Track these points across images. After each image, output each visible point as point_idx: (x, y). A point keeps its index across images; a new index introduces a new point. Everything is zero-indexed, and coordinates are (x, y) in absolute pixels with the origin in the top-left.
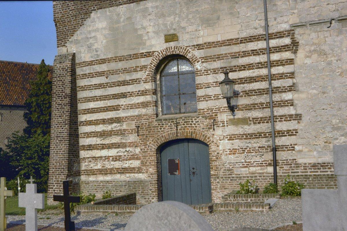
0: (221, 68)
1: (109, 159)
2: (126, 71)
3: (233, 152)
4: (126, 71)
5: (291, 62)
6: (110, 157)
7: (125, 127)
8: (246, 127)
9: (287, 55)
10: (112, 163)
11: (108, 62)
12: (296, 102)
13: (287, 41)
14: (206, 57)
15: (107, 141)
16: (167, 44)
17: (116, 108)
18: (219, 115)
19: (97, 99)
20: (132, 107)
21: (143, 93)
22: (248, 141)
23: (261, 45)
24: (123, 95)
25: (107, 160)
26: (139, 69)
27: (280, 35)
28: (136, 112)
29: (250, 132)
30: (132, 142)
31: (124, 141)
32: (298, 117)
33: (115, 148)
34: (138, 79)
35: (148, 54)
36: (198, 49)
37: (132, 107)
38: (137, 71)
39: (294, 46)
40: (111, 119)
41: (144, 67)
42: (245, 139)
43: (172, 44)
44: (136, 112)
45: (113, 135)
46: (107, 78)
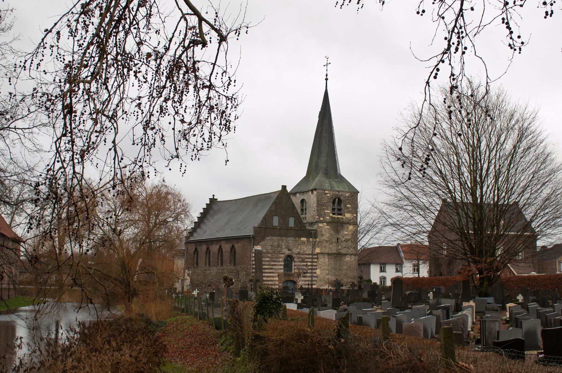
5: (316, 262)
9: (316, 260)
13: (316, 257)
15: (269, 279)
21: (281, 265)
27: (315, 255)
32: (317, 277)
39: (317, 258)
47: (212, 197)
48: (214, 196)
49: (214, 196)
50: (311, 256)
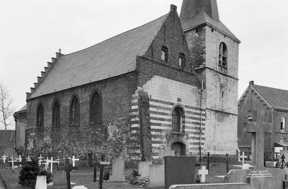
0: (191, 117)
1: (156, 148)
2: (164, 108)
3: (191, 149)
4: (164, 108)
6: (156, 147)
7: (162, 134)
8: (194, 140)
9: (204, 117)
10: (157, 150)
11: (159, 102)
12: (205, 134)
14: (188, 111)
16: (178, 102)
17: (160, 125)
18: (189, 134)
19: (153, 118)
20: (165, 125)
22: (195, 145)
23: (198, 112)
24: (163, 120)
25: (155, 149)
26: (169, 109)
28: (166, 128)
29: (195, 142)
30: (164, 142)
31: (162, 141)
33: (159, 143)
34: (168, 113)
35: (172, 104)
36: (186, 108)
37: (165, 125)
38: (168, 110)
40: (158, 129)
41: (170, 109)
42: (194, 145)
43: (179, 102)
44: (166, 128)
45: (158, 137)
46: (158, 109)
47: (58, 52)
48: (60, 50)
49: (60, 50)
50: (198, 112)
